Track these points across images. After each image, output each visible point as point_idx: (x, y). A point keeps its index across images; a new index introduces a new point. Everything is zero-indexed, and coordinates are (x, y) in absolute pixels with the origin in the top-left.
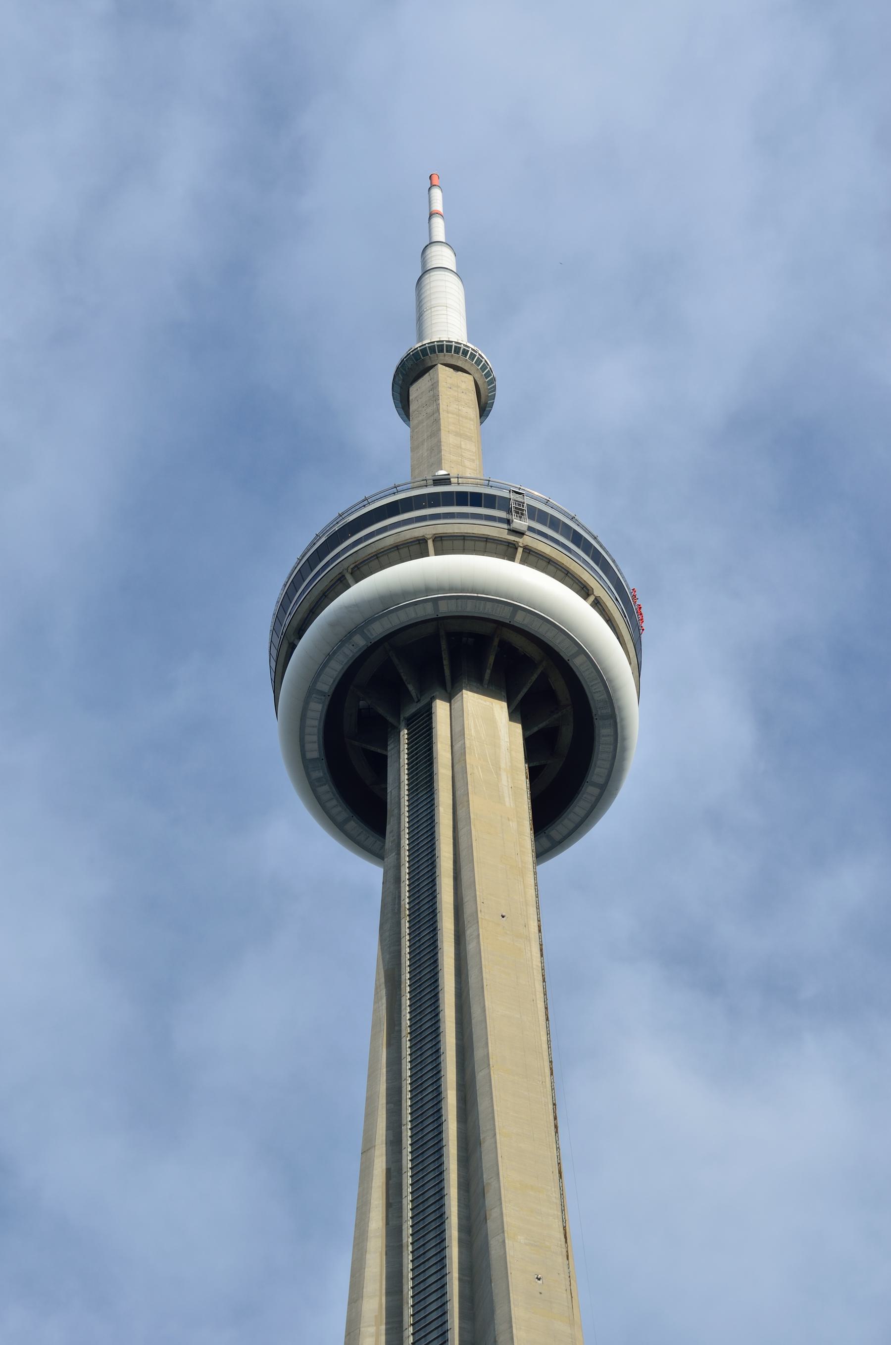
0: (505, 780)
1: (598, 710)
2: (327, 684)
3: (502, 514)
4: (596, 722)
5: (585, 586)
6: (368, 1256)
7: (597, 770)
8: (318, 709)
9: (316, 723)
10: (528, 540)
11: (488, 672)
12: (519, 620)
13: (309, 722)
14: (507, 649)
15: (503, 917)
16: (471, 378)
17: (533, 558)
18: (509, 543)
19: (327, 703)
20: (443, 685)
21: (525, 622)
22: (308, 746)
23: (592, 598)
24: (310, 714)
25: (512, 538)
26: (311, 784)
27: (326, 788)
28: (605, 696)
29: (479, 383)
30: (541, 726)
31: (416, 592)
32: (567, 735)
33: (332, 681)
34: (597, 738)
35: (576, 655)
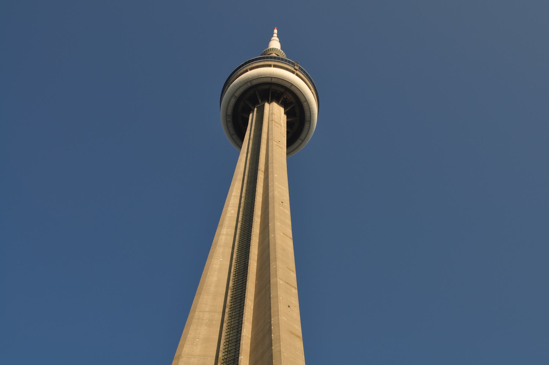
0: (282, 121)
2: (238, 94)
8: (233, 100)
10: (298, 72)
11: (280, 102)
25: (294, 70)
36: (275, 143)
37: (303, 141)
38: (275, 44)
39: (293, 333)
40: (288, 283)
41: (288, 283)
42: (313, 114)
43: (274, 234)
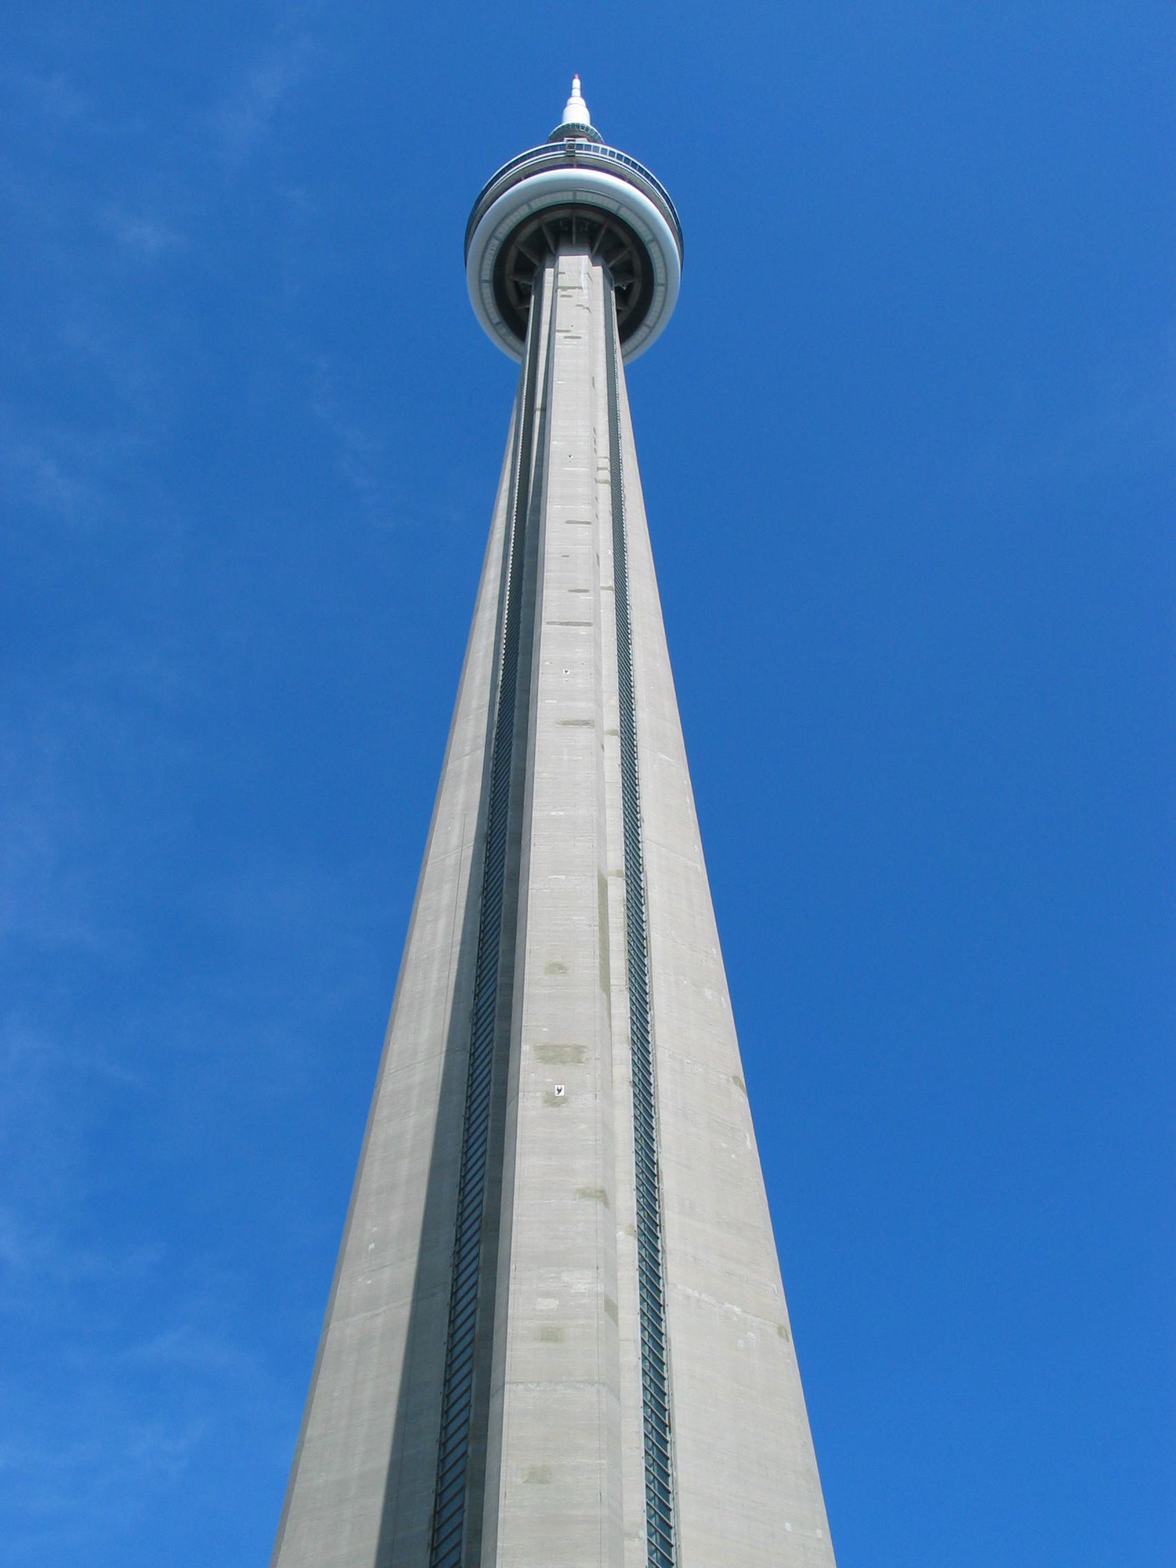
14: (581, 221)
32: (637, 264)
37: (666, 285)
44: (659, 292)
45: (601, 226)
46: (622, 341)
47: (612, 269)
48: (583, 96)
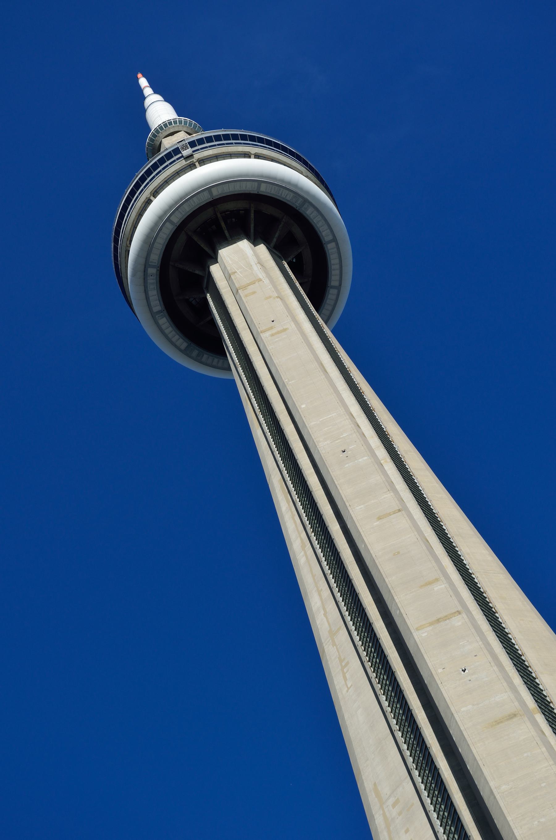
1: (296, 204)
2: (157, 306)
3: (180, 155)
4: (301, 211)
5: (245, 154)
6: (287, 524)
7: (324, 234)
8: (164, 321)
9: (170, 329)
10: (197, 156)
12: (216, 193)
13: (167, 331)
15: (273, 321)
16: (183, 132)
17: (203, 162)
18: (190, 165)
19: (167, 315)
20: (212, 258)
21: (220, 192)
22: (178, 343)
23: (253, 156)
24: (164, 327)
26: (196, 360)
27: (205, 356)
28: (292, 194)
29: (188, 131)
30: (277, 235)
31: (156, 224)
32: (297, 231)
33: (158, 302)
34: (308, 218)
35: (259, 187)
36: (267, 334)
37: (334, 239)
38: (159, 111)
39: (498, 722)
40: (438, 621)
41: (438, 621)
42: (296, 186)
43: (363, 541)
44: (330, 248)
45: (247, 211)
46: (317, 310)
47: (275, 247)
48: (156, 92)
